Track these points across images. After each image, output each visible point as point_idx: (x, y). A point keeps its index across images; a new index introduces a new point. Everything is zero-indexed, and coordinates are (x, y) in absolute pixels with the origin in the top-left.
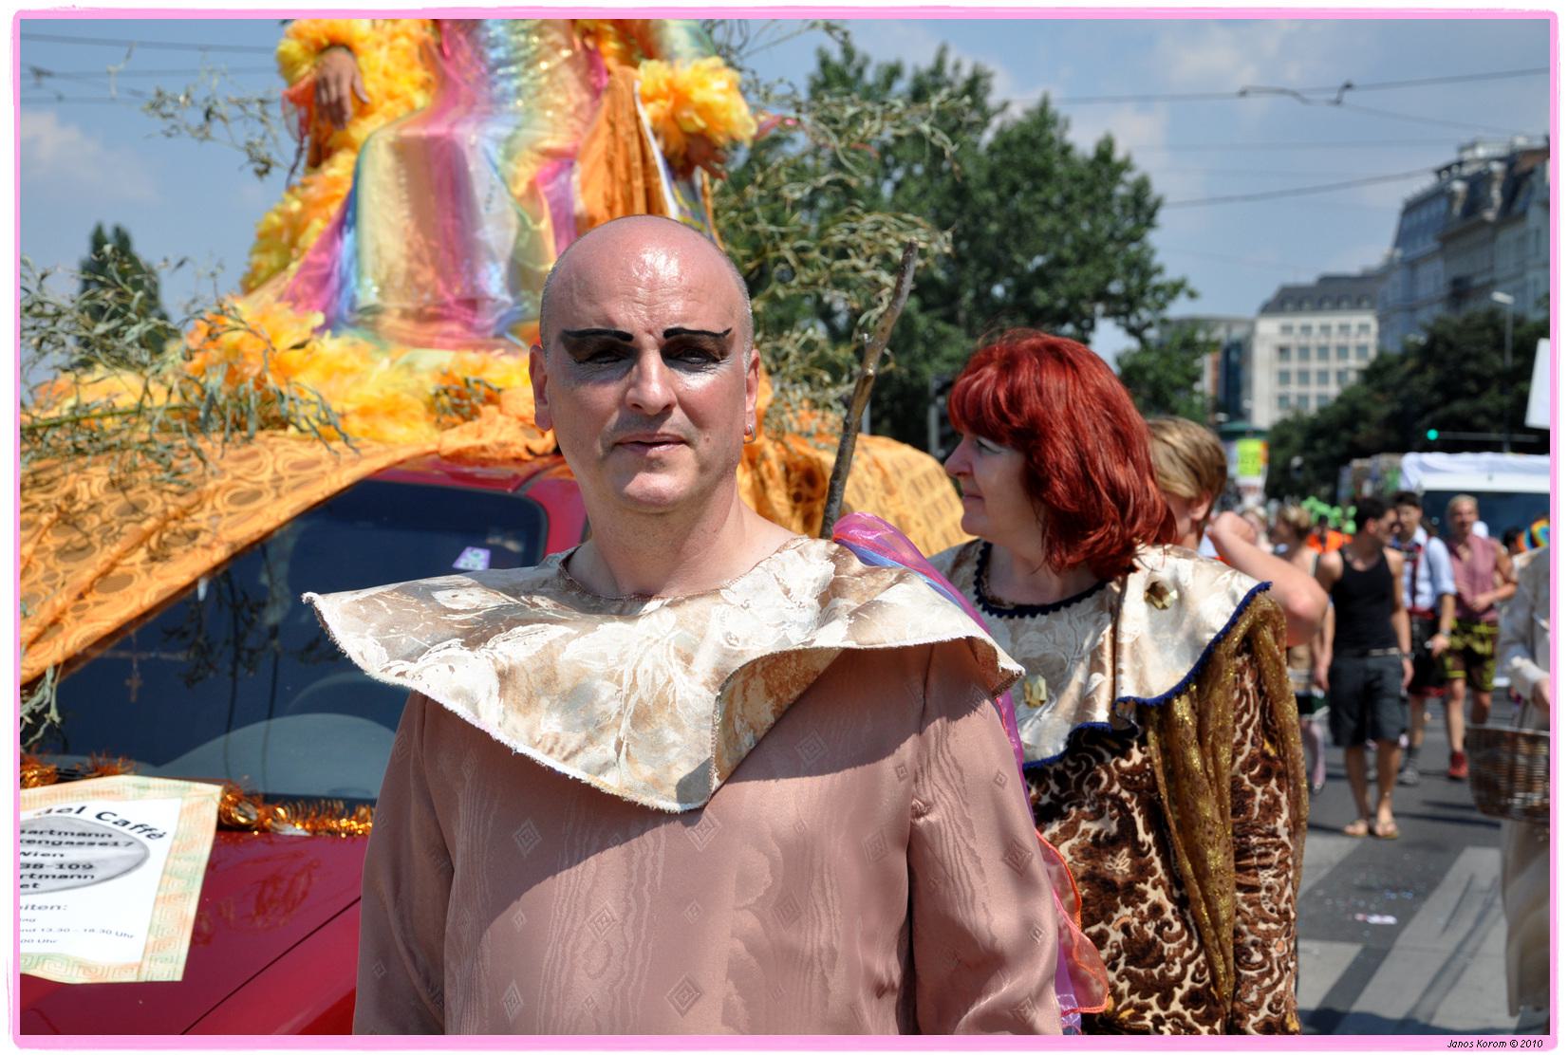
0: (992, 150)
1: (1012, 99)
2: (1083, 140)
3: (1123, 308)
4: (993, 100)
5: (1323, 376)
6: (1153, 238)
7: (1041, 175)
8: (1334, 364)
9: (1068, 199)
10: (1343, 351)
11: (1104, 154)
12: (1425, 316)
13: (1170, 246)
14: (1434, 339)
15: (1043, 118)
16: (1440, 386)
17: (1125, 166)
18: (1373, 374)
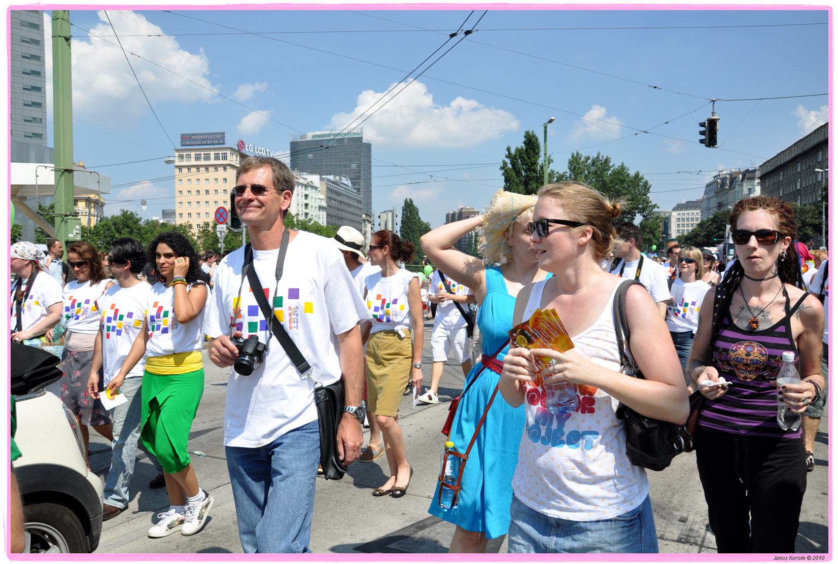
0: (611, 175)
1: (615, 163)
2: (632, 173)
3: (642, 211)
4: (611, 164)
5: (683, 225)
6: (648, 195)
7: (622, 182)
8: (690, 222)
9: (629, 186)
10: (692, 219)
11: (637, 175)
12: (712, 211)
13: (653, 197)
14: (715, 217)
15: (623, 168)
16: (716, 228)
17: (642, 178)
18: (700, 225)
